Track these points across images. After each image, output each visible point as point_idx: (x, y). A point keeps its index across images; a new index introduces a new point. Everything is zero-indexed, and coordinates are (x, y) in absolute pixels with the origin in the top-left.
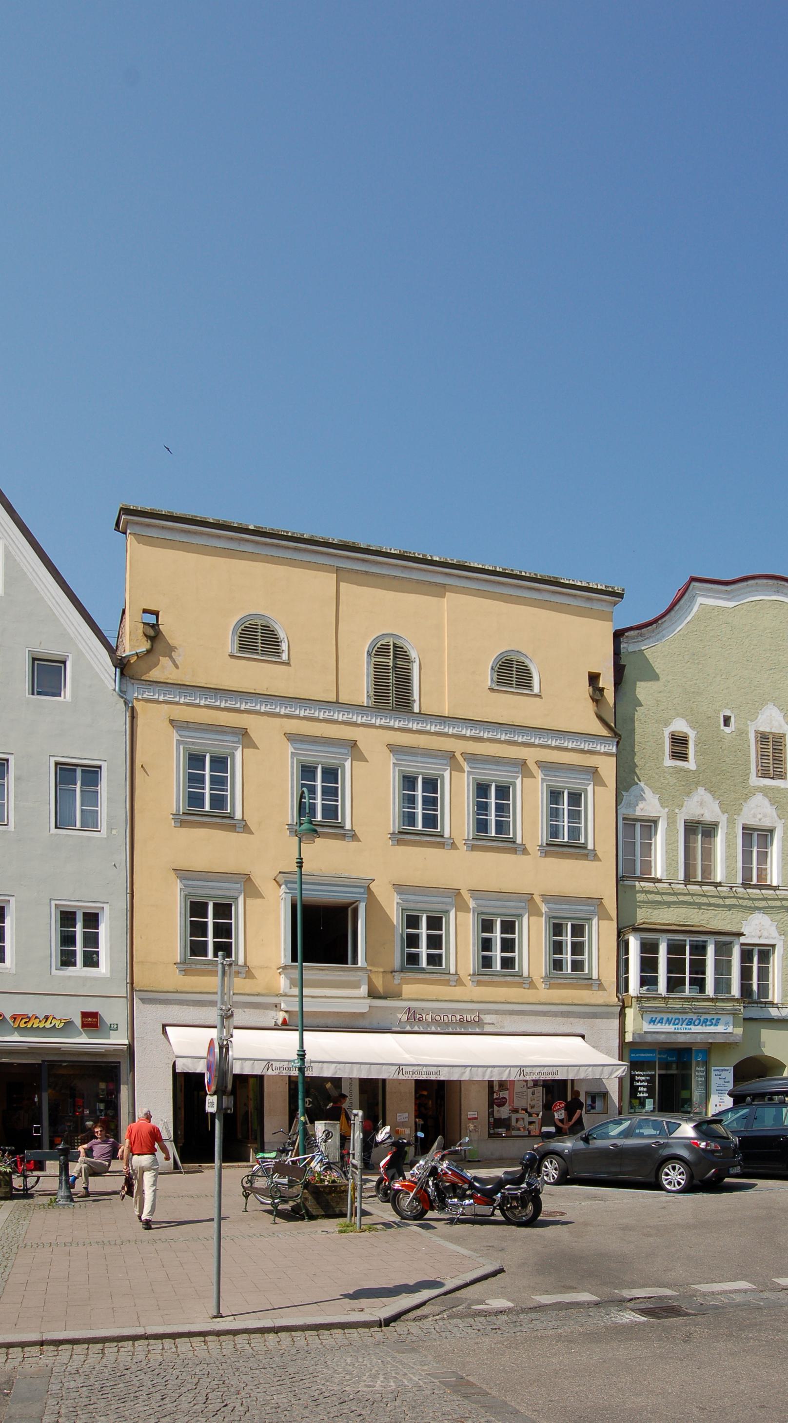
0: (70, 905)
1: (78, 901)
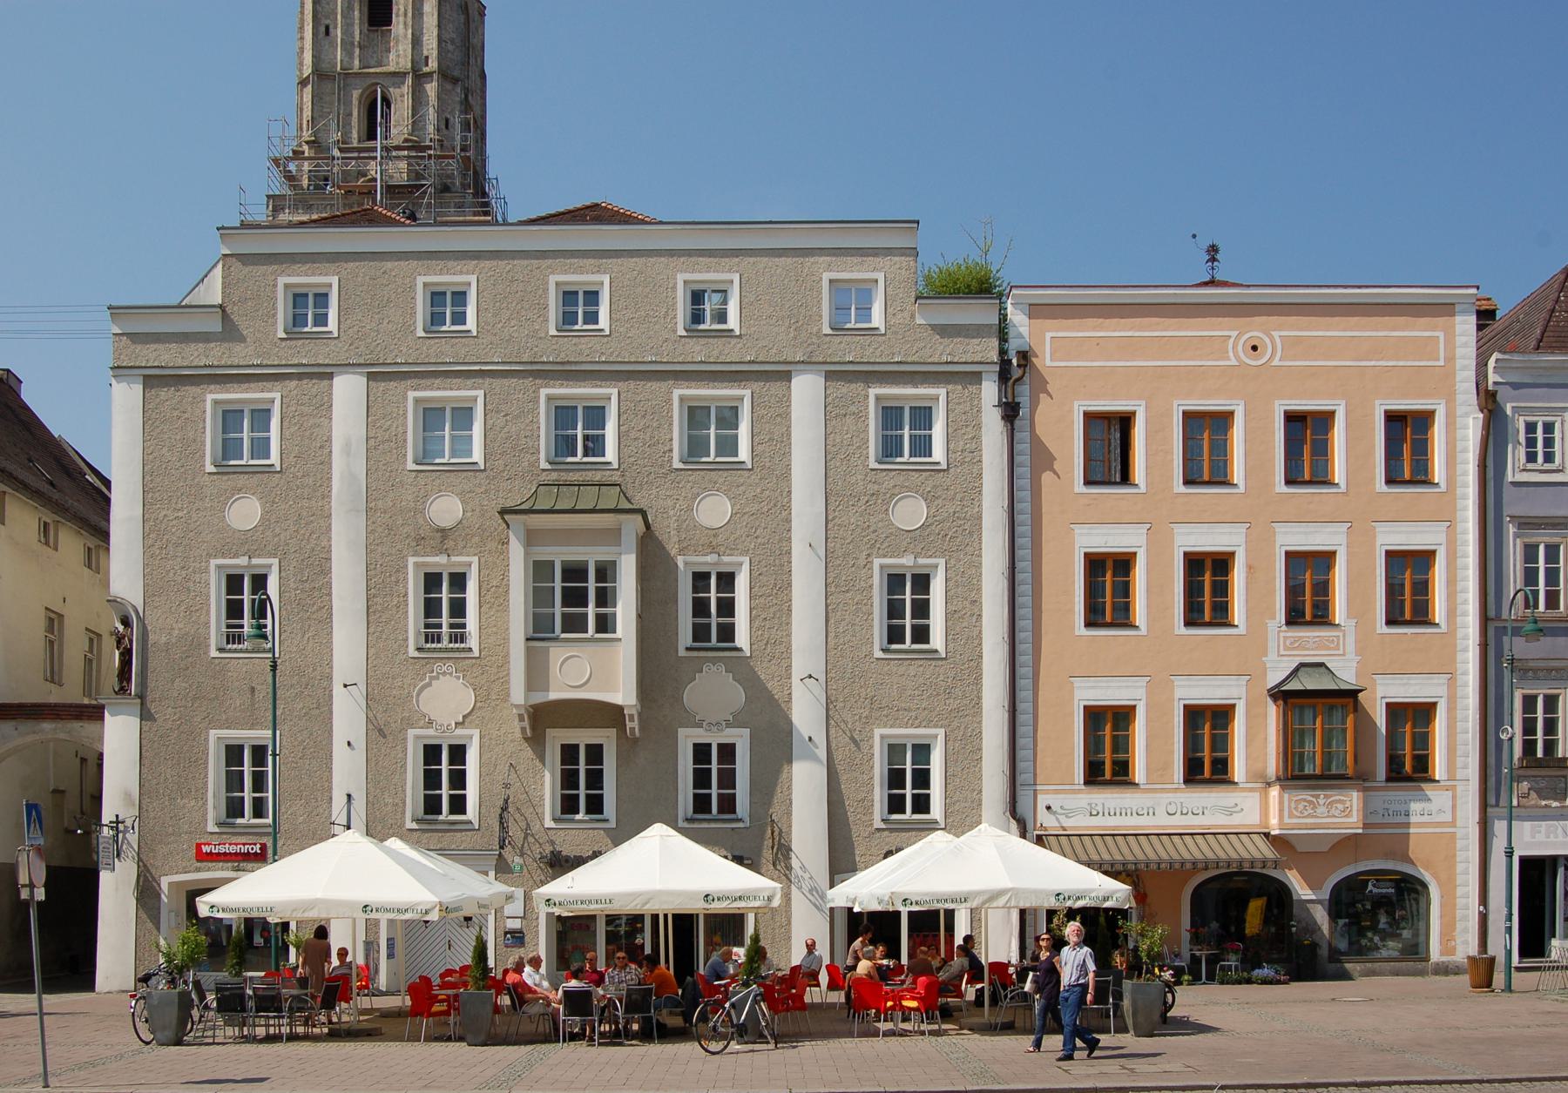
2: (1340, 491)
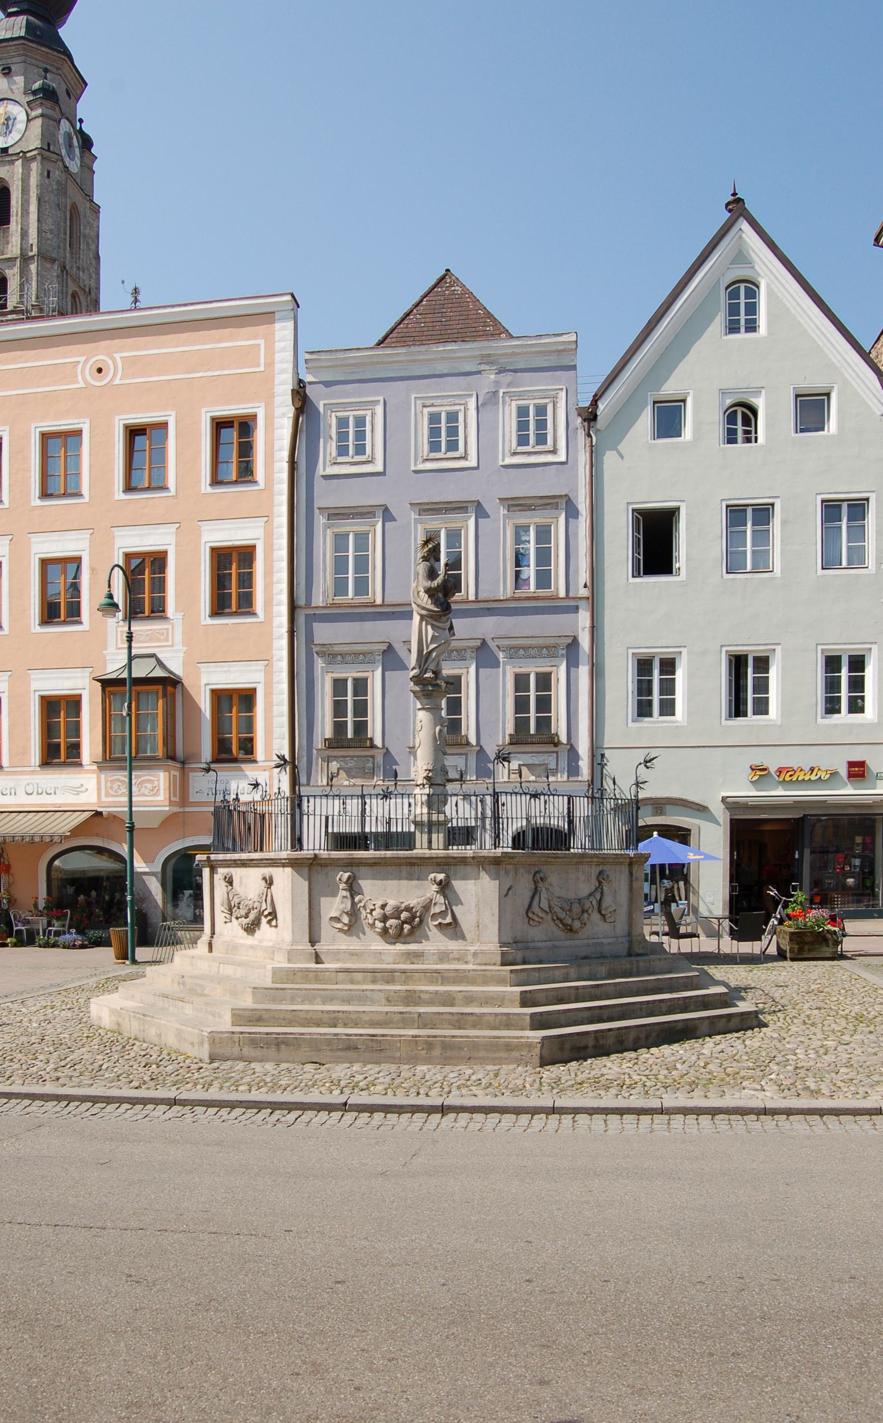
0: (834, 649)
1: (845, 644)
2: (170, 494)
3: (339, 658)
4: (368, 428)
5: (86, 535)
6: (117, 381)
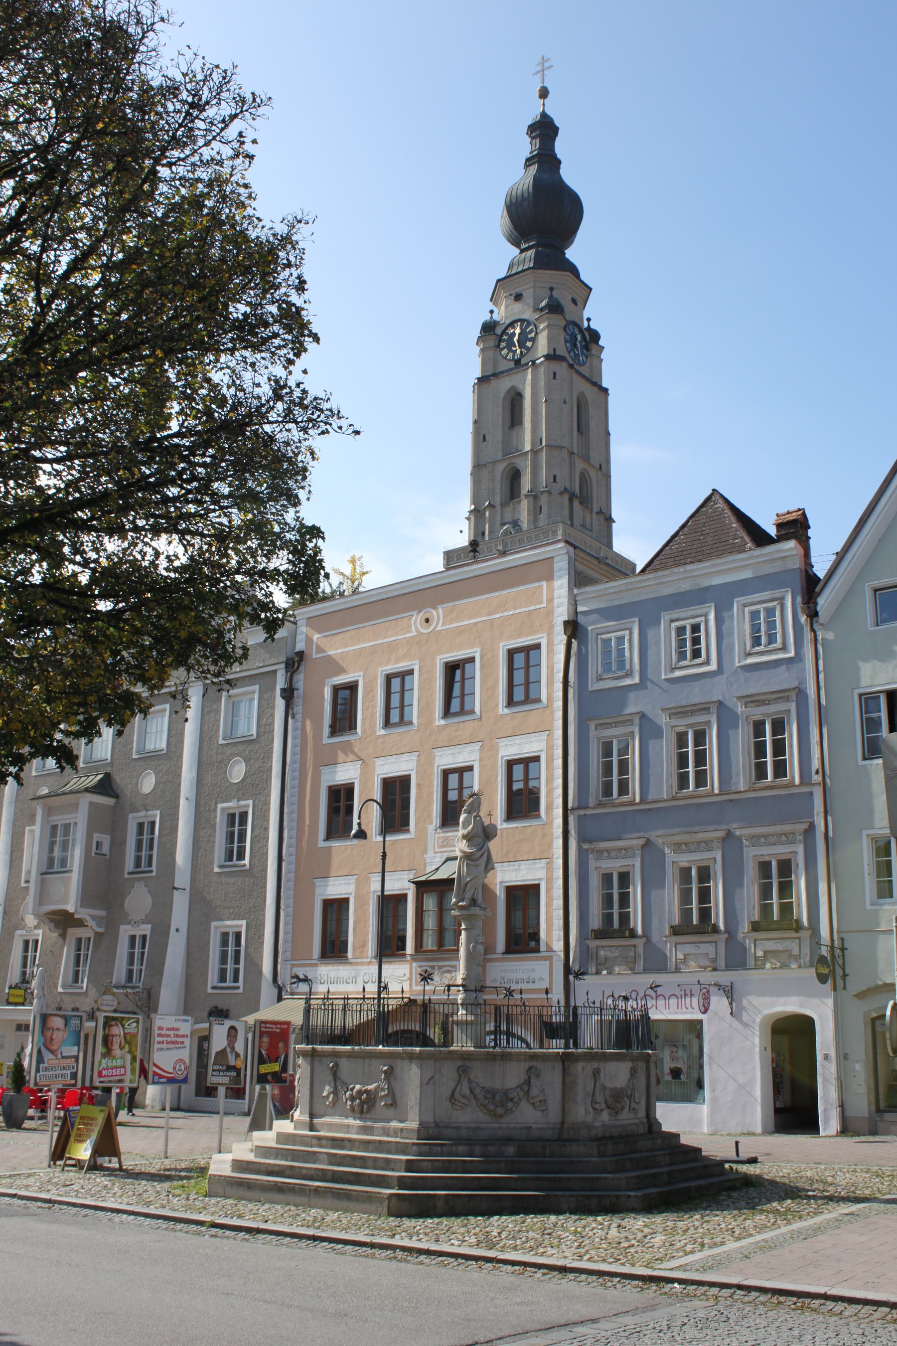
3: (606, 854)
4: (627, 645)
5: (414, 756)
6: (439, 628)
